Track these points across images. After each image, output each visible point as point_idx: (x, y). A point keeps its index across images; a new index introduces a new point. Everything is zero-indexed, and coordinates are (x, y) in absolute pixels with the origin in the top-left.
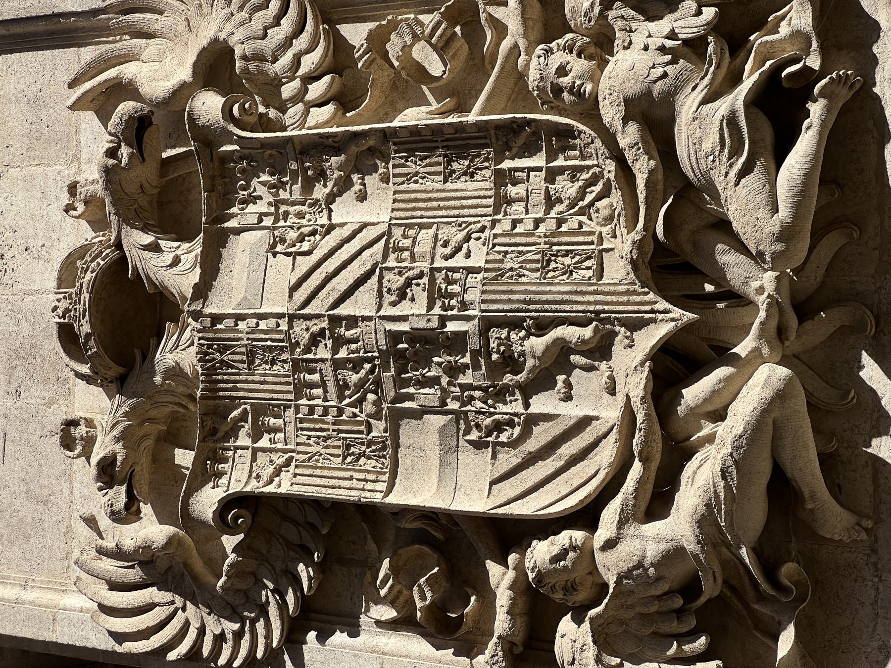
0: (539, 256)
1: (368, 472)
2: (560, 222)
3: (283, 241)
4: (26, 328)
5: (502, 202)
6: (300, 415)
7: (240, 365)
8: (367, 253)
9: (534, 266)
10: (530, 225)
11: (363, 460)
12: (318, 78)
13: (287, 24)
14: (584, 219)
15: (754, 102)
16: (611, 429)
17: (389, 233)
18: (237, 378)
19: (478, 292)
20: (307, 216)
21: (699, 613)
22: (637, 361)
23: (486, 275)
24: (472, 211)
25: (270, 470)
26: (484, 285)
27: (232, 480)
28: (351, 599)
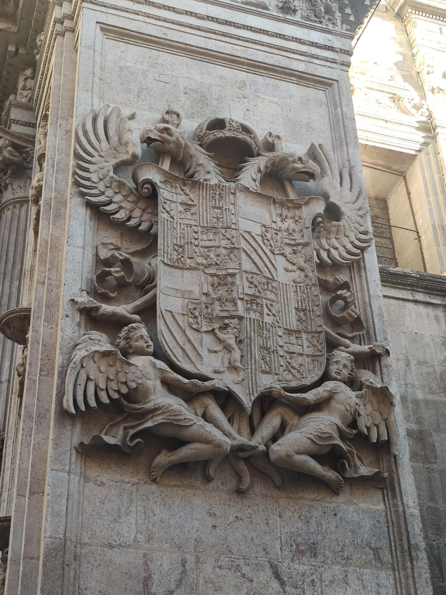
0: (269, 346)
2: (282, 356)
3: (267, 231)
4: (215, 103)
5: (289, 332)
7: (214, 203)
8: (266, 269)
10: (281, 344)
11: (176, 253)
12: (329, 257)
13: (350, 247)
14: (284, 368)
17: (274, 280)
19: (254, 317)
20: (277, 244)
22: (229, 385)
23: (261, 322)
24: (284, 319)
25: (168, 209)
28: (105, 237)
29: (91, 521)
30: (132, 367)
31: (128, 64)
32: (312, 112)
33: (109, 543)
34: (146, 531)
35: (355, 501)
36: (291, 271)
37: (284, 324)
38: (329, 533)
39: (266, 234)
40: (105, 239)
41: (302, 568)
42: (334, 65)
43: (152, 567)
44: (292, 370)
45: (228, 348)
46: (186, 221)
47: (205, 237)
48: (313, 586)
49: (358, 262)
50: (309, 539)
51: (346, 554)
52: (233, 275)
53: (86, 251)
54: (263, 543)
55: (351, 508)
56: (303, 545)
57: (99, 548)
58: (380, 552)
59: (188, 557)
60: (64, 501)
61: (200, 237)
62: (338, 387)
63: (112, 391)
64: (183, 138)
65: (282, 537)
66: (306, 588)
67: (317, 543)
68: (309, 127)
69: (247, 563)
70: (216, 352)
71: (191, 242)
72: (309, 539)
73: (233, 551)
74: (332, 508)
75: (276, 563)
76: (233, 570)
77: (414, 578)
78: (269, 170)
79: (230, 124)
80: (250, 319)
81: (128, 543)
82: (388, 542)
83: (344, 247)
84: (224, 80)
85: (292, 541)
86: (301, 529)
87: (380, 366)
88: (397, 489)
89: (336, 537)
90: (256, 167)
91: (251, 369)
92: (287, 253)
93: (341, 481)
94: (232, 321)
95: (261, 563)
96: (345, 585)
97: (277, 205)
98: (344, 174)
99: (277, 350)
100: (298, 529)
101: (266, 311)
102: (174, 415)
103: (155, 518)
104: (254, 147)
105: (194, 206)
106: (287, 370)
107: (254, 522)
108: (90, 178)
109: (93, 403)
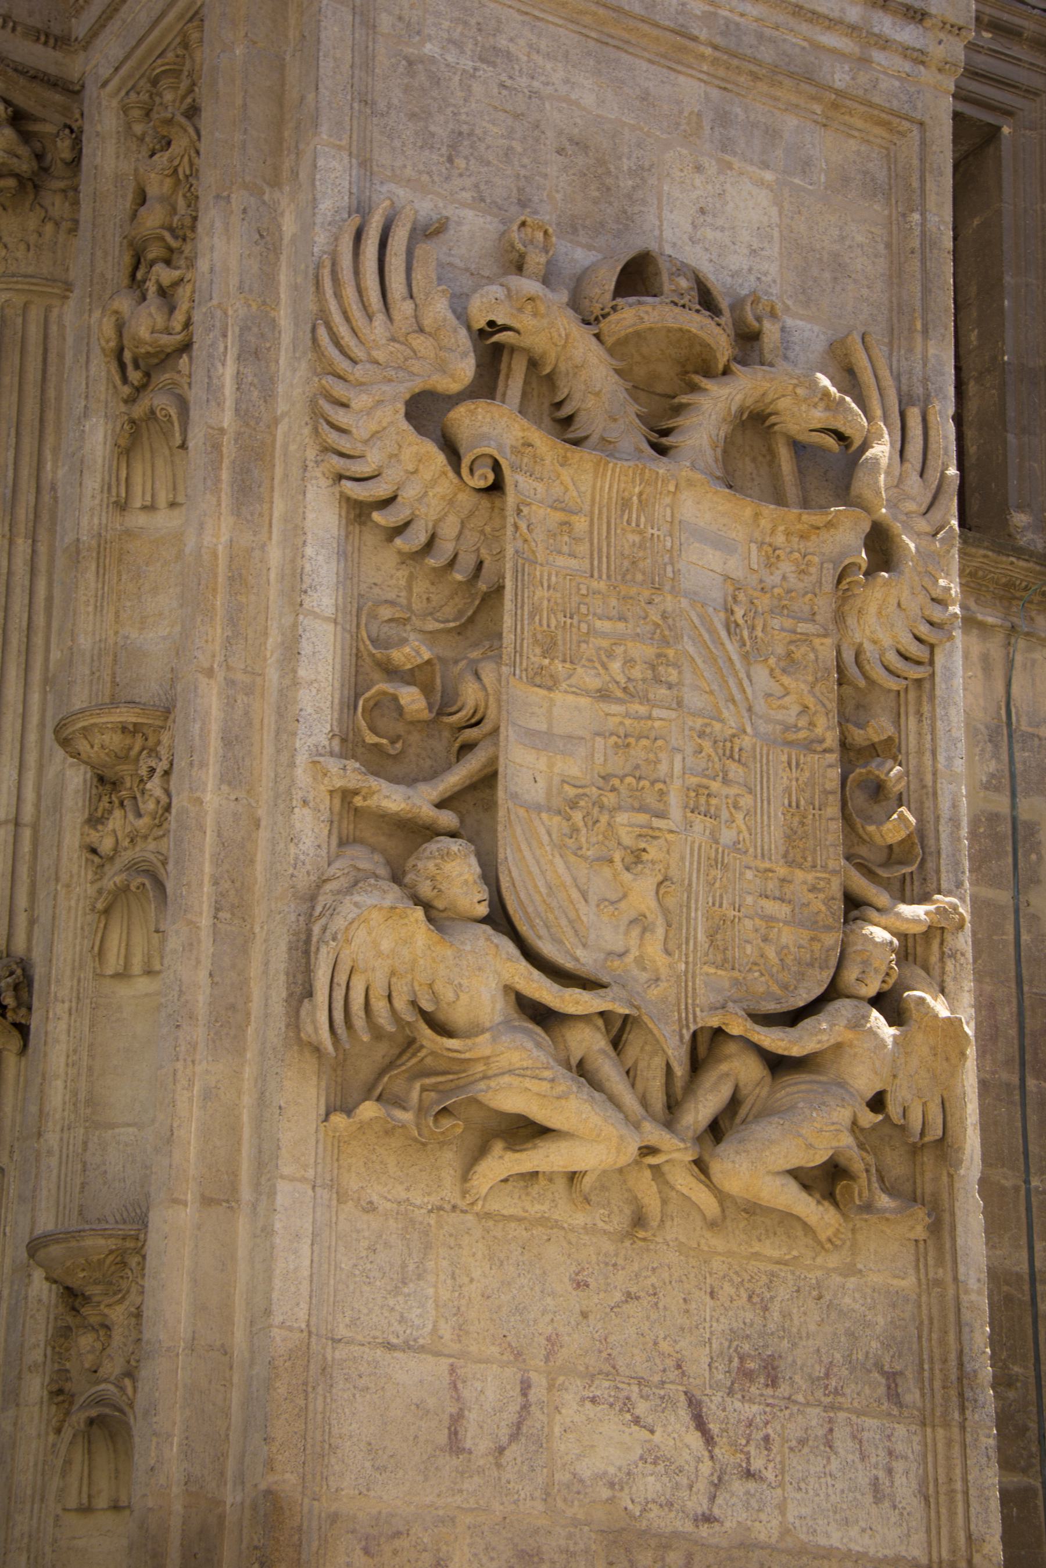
29: (351, 1288)
38: (804, 1335)
43: (467, 1393)
56: (753, 1358)
58: (899, 1380)
59: (533, 1376)
65: (714, 1341)
66: (753, 1453)
72: (766, 1346)
77: (964, 1446)
82: (917, 1362)
86: (751, 1325)
88: (948, 1246)
103: (473, 1286)
107: (661, 1305)
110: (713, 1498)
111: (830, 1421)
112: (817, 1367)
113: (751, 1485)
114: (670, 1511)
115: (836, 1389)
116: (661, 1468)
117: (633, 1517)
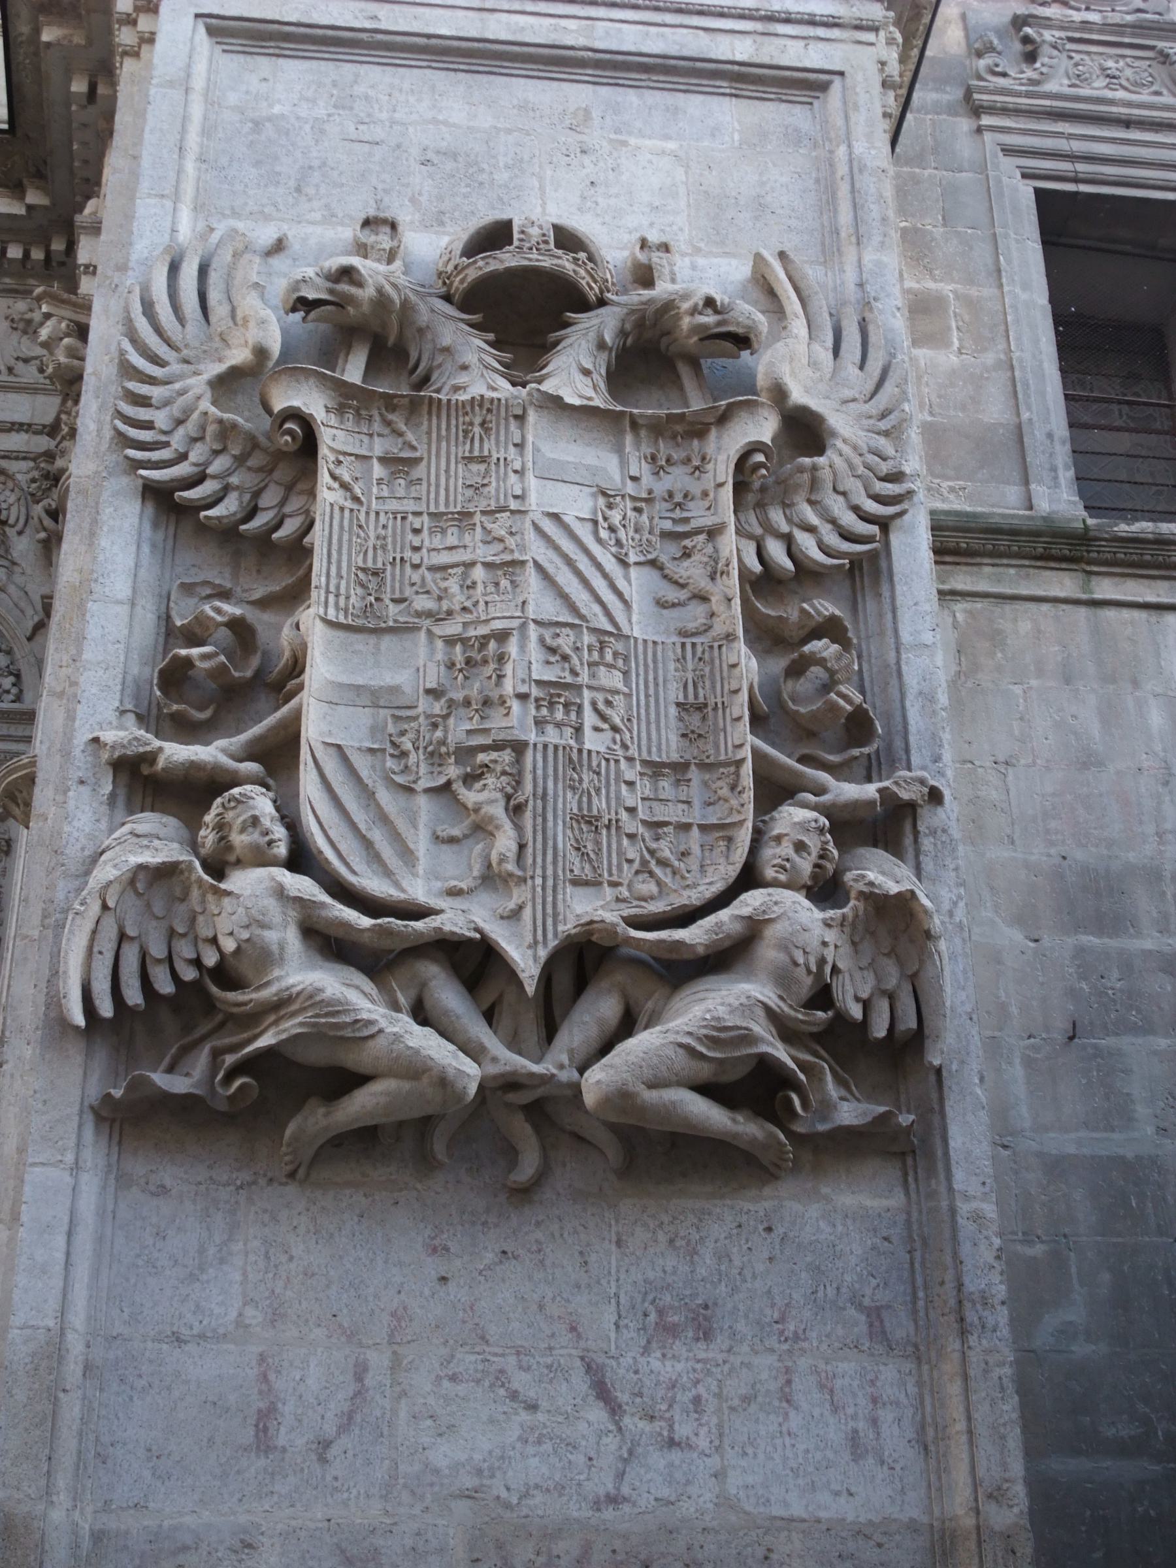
0: (595, 812)
1: (348, 598)
2: (631, 837)
3: (610, 506)
4: (502, 176)
5: (655, 769)
6: (410, 517)
7: (468, 447)
8: (597, 608)
9: (585, 806)
10: (630, 803)
11: (359, 591)
12: (790, 554)
13: (849, 519)
14: (636, 865)
15: (765, 1066)
16: (403, 891)
17: (620, 636)
18: (453, 443)
19: (556, 741)
20: (637, 537)
21: (197, 985)
22: (481, 924)
23: (575, 751)
24: (644, 735)
25: (347, 478)
26: (564, 748)
27: (334, 431)
28: (194, 566)
29: (133, 1281)
30: (226, 901)
31: (277, 110)
32: (770, 165)
33: (173, 1333)
34: (267, 1298)
35: (825, 1190)
36: (674, 605)
37: (644, 749)
38: (748, 1275)
39: (609, 513)
40: (193, 571)
41: (669, 1370)
42: (835, 33)
44: (658, 871)
45: (482, 829)
46: (393, 505)
47: (437, 542)
48: (696, 1412)
49: (873, 556)
50: (694, 1296)
51: (792, 1328)
52: (502, 636)
53: (138, 609)
54: (571, 1314)
55: (814, 1211)
57: (149, 1344)
58: (885, 1314)
60: (60, 1241)
61: (427, 543)
62: (776, 903)
63: (182, 963)
64: (394, 286)
65: (622, 1296)
66: (677, 1418)
67: (715, 1304)
68: (760, 207)
69: (524, 1364)
70: (452, 840)
71: (402, 559)
72: (694, 1296)
73: (488, 1337)
74: (762, 1214)
75: (600, 1361)
76: (487, 1384)
78: (629, 341)
79: (523, 232)
80: (545, 746)
81: (221, 1331)
82: (909, 1291)
83: (833, 522)
84: (531, 114)
85: (646, 1304)
86: (674, 1273)
87: (916, 833)
89: (767, 1287)
90: (592, 335)
91: (544, 878)
92: (664, 559)
93: (779, 1143)
94: (494, 755)
95: (562, 1361)
96: (785, 1404)
97: (643, 433)
98: (845, 323)
99: (617, 821)
100: (665, 1272)
101: (589, 718)
102: (327, 1015)
103: (293, 1266)
104: (588, 284)
105: (417, 461)
106: (644, 869)
107: (548, 1263)
108: (152, 422)
109: (134, 996)
110: (621, 1476)
111: (788, 1370)
112: (768, 1312)
113: (676, 1456)
114: (561, 1495)
115: (796, 1333)
116: (547, 1447)
117: (508, 1506)
